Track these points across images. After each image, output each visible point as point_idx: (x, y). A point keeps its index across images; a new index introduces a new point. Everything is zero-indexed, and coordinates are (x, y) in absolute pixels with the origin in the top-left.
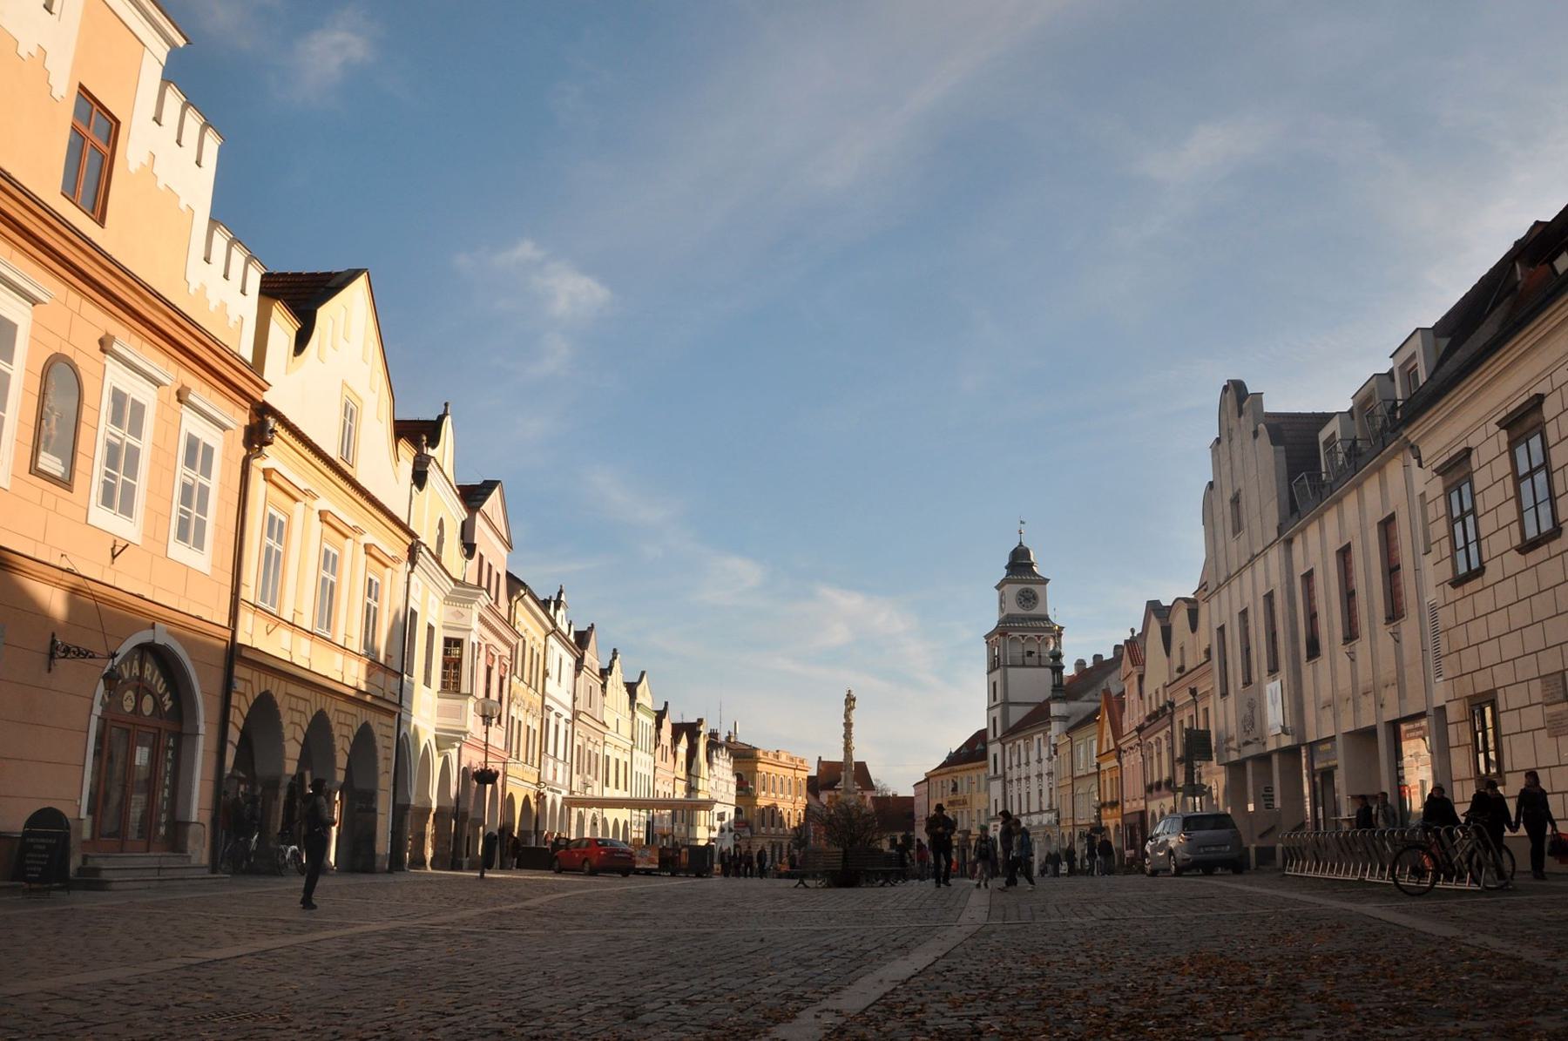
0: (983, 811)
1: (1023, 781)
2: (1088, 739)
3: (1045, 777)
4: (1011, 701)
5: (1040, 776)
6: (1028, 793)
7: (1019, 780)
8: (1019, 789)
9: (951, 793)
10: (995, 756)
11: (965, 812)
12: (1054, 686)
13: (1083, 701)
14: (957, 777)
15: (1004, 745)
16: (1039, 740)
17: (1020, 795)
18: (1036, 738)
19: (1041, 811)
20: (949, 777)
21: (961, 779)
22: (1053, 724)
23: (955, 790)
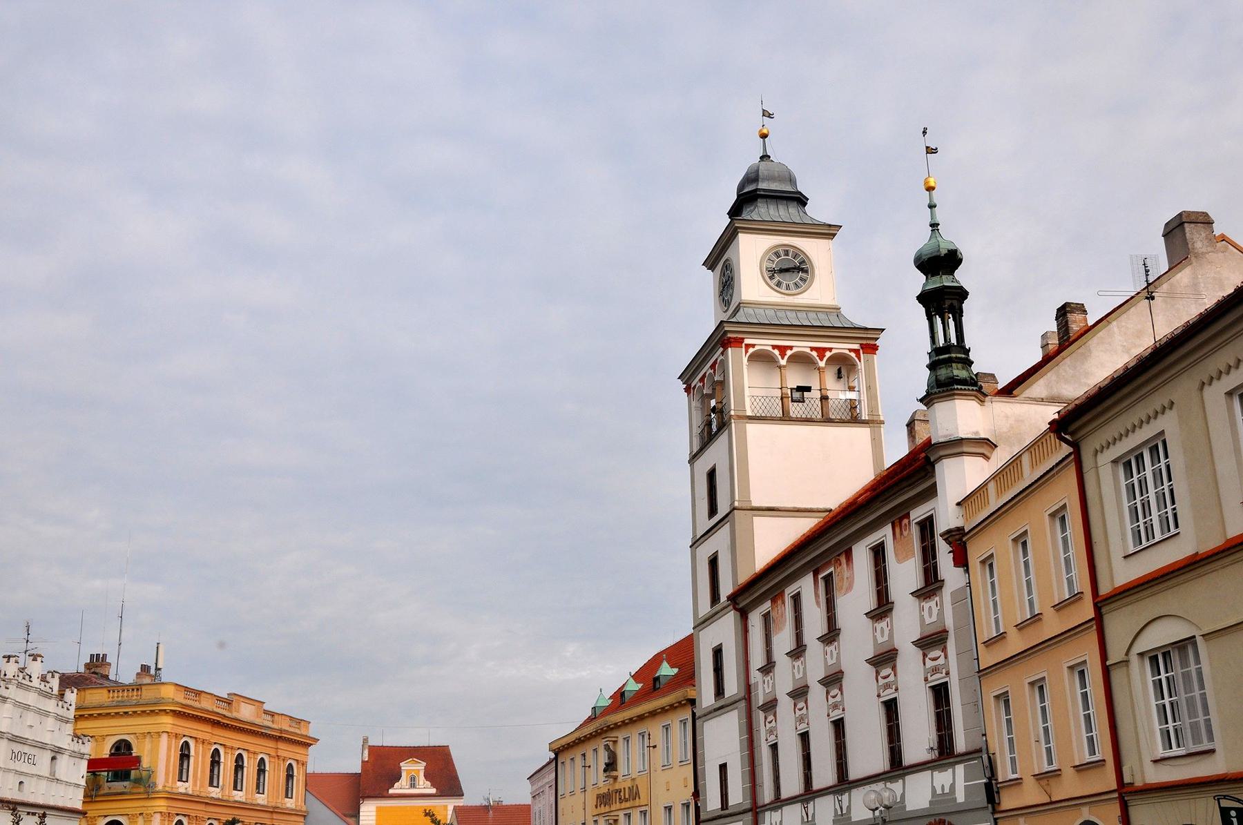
0: (678, 811)
1: (817, 693)
2: (1215, 394)
3: (910, 659)
4: (755, 504)
5: (885, 659)
6: (839, 726)
7: (800, 693)
8: (801, 719)
9: (602, 776)
10: (718, 653)
11: (636, 816)
12: (937, 351)
13: (1042, 400)
14: (615, 742)
15: (744, 614)
16: (878, 552)
17: (805, 737)
18: (861, 554)
19: (897, 767)
20: (600, 744)
21: (627, 740)
22: (937, 466)
23: (611, 766)
